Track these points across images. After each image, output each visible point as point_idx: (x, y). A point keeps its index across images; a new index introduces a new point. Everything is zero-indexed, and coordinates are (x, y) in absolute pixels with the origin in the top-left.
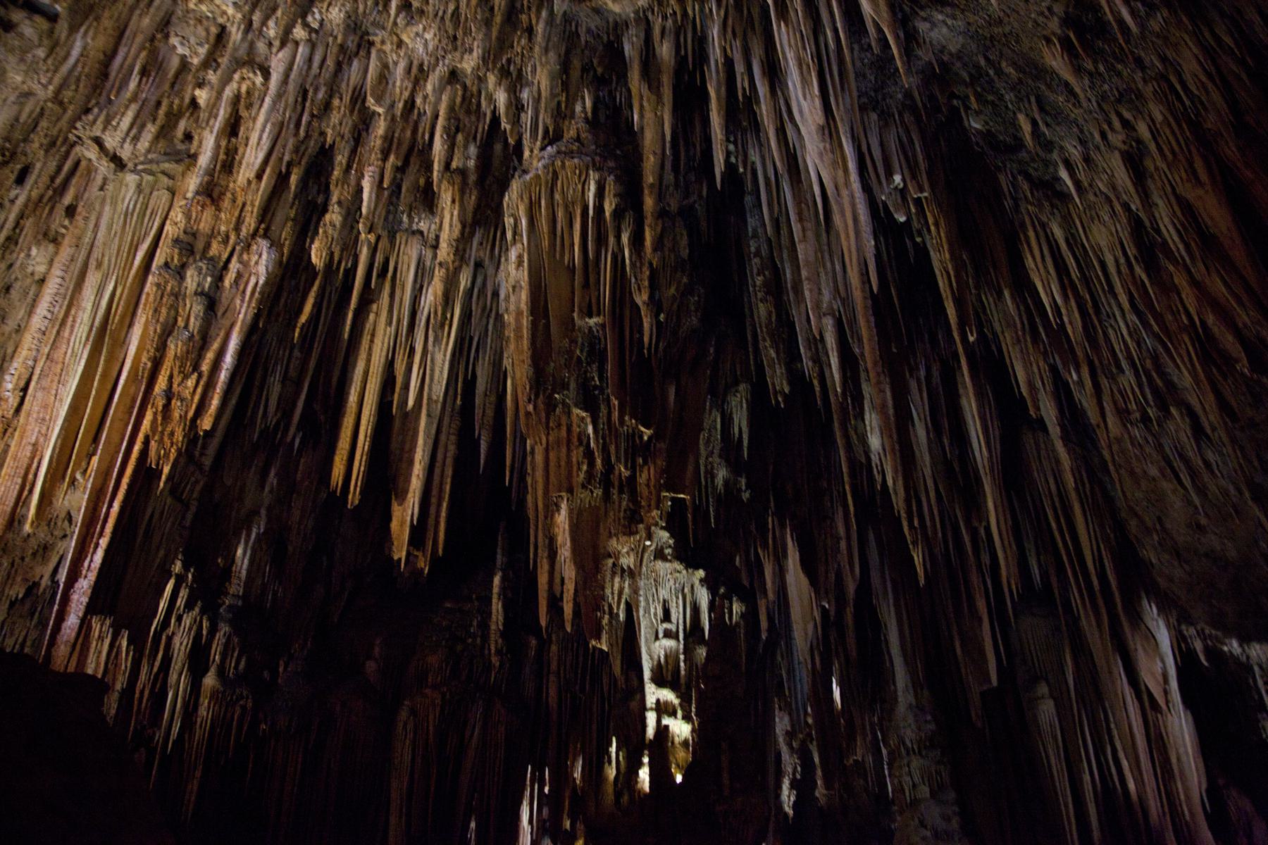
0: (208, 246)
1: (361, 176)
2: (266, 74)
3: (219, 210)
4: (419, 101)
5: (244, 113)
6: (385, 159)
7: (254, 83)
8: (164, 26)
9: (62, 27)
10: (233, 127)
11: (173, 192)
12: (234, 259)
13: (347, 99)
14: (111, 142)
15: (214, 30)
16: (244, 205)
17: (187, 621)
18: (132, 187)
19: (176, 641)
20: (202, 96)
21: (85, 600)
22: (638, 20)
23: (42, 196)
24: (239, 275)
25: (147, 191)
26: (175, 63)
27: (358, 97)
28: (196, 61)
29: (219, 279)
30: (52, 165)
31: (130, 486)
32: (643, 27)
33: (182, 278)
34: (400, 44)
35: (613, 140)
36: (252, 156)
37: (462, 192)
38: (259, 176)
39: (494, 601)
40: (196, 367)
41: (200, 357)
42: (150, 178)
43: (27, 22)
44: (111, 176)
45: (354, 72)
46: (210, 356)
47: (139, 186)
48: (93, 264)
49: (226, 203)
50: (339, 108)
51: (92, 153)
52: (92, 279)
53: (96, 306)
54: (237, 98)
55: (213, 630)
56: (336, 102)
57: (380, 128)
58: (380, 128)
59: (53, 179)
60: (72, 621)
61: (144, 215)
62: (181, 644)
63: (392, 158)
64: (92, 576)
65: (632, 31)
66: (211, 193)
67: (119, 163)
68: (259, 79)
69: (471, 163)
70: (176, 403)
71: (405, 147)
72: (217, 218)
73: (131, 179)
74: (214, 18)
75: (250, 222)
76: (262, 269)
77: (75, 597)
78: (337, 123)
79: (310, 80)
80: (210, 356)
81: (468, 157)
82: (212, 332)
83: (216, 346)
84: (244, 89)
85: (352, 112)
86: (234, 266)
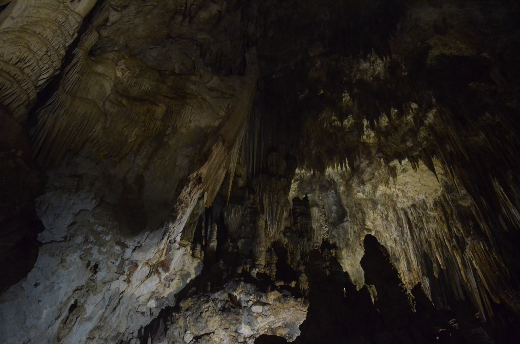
1: (436, 255)
27: (426, 239)
35: (480, 234)
37: (457, 251)
38: (418, 266)
45: (423, 236)
57: (433, 243)
58: (433, 243)
65: (472, 208)
69: (455, 243)
75: (421, 274)
76: (427, 283)
78: (425, 247)
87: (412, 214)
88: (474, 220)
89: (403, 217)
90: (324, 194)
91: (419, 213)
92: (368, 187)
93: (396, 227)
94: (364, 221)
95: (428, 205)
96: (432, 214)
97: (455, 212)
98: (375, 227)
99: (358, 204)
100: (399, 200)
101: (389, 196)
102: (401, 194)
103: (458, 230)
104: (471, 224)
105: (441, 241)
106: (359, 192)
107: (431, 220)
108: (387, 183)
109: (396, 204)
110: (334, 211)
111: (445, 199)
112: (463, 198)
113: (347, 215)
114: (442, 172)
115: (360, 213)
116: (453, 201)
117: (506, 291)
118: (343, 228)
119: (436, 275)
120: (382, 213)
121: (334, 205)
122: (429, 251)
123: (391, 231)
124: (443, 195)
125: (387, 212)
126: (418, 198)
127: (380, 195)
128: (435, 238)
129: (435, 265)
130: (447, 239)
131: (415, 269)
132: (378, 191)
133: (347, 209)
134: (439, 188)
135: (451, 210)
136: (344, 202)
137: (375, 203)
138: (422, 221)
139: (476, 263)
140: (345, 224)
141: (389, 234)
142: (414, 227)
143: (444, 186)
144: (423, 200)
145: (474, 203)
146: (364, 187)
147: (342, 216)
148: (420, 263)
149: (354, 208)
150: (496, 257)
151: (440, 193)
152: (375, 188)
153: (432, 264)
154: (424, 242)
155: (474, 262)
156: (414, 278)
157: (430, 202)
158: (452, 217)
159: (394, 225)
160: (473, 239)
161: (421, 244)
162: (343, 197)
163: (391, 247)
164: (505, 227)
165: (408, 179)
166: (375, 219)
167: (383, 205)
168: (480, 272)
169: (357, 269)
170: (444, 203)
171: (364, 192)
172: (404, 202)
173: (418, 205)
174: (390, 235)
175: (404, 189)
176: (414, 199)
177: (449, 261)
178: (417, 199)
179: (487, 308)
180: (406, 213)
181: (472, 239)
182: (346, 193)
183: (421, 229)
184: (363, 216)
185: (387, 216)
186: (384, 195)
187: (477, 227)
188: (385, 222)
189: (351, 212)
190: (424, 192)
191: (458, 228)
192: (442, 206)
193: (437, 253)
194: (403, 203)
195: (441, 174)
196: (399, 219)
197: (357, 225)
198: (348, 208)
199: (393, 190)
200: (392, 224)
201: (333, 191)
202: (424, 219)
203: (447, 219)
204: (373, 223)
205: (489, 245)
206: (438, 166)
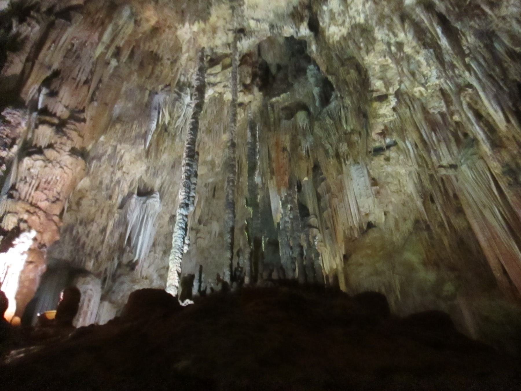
2: (470, 86)
3: (506, 148)
5: (477, 107)
7: (470, 94)
8: (424, 110)
9: (401, 144)
10: (478, 116)
11: (482, 158)
13: (508, 59)
14: (444, 163)
15: (439, 93)
16: (514, 137)
20: (456, 118)
26: (439, 117)
28: (444, 109)
30: (437, 189)
34: (504, 18)
36: (498, 117)
38: (508, 121)
42: (469, 161)
43: (391, 152)
44: (456, 173)
47: (469, 167)
48: (482, 208)
49: (506, 142)
50: (509, 65)
51: (443, 172)
54: (470, 106)
56: (506, 65)
59: (441, 191)
61: (481, 176)
66: (497, 143)
67: (453, 167)
68: (470, 90)
72: (509, 151)
73: (464, 168)
74: (435, 90)
79: (487, 69)
84: (468, 99)
90: (302, 80)
98: (388, 84)
115: (352, 71)
120: (389, 44)
121: (317, 86)
140: (333, 104)
146: (327, 6)
189: (338, 80)
197: (350, 94)
198: (332, 74)
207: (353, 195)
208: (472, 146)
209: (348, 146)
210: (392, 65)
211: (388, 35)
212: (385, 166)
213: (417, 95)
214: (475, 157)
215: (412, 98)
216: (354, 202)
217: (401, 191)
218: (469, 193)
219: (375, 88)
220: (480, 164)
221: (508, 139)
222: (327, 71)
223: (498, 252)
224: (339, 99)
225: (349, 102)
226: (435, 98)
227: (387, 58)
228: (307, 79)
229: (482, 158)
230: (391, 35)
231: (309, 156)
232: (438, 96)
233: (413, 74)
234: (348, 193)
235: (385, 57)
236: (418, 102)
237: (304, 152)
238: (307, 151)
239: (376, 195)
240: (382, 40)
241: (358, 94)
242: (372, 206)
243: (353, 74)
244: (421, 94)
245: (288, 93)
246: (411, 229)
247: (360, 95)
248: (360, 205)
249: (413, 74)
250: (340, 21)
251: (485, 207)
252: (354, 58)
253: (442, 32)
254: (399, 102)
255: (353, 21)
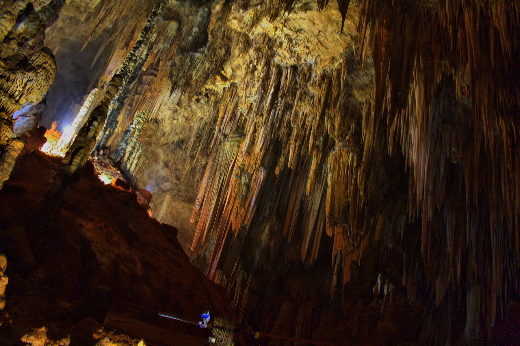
0: (248, 169)
1: (290, 147)
4: (307, 122)
6: (296, 142)
8: (236, 106)
12: (255, 173)
15: (249, 105)
17: (241, 273)
18: (228, 146)
19: (238, 279)
21: (216, 266)
22: (366, 103)
23: (205, 147)
24: (256, 178)
25: (232, 147)
27: (289, 123)
29: (250, 179)
31: (227, 236)
32: (367, 105)
33: (241, 179)
37: (317, 153)
38: (261, 150)
39: (334, 275)
40: (244, 206)
41: (245, 202)
45: (287, 117)
46: (248, 202)
52: (218, 173)
53: (219, 182)
55: (248, 276)
56: (282, 125)
58: (295, 132)
60: (213, 271)
62: (239, 280)
63: (298, 142)
64: (218, 260)
65: (364, 106)
66: (249, 152)
67: (225, 136)
69: (321, 144)
70: (239, 216)
71: (301, 139)
75: (259, 162)
76: (262, 176)
77: (214, 265)
78: (283, 131)
80: (248, 202)
81: (320, 142)
82: (249, 195)
83: (249, 199)
85: (287, 128)
86: (254, 175)
87: (286, 78)
88: (359, 124)
89: (273, 77)
90: (194, 8)
91: (296, 82)
92: (248, 16)
93: (258, 88)
94: (223, 61)
95: (313, 75)
96: (311, 90)
97: (341, 100)
98: (233, 76)
99: (228, 38)
100: (280, 51)
101: (270, 40)
102: (285, 45)
103: (333, 126)
104: (353, 127)
105: (305, 134)
106: (235, 18)
107: (307, 99)
108: (274, 17)
109: (273, 55)
110: (193, 34)
111: (338, 77)
112: (362, 88)
113: (206, 45)
114: (355, 33)
115: (223, 50)
116: (346, 84)
117: (346, 225)
118: (192, 60)
119: (277, 172)
120: (251, 62)
122: (284, 140)
123: (251, 91)
124: (339, 72)
125: (257, 62)
126: (305, 60)
127: (259, 34)
128: (300, 127)
129: (282, 159)
130: (314, 133)
131: (256, 152)
132: (259, 27)
133: (210, 37)
134: (338, 57)
135: (338, 95)
136: (211, 27)
137: (248, 43)
138: (294, 95)
139: (332, 177)
140: (198, 55)
141: (246, 94)
142: (280, 94)
143: (346, 57)
144: (311, 65)
145: (373, 103)
147: (200, 42)
148: (266, 150)
149: (219, 41)
150: (359, 179)
151: (336, 64)
152: (256, 21)
153: (280, 157)
154: (284, 125)
155: (330, 176)
156: (249, 164)
157: (318, 72)
158: (335, 106)
159: (257, 85)
160: (344, 146)
161: (280, 126)
162: (213, 19)
163: (241, 114)
164: (390, 148)
165: (305, 25)
166: (239, 67)
167: (258, 50)
168: (329, 191)
169: (191, 127)
170: (334, 80)
171: (240, 20)
172: (285, 57)
173: (300, 69)
174: (246, 96)
175: (293, 38)
176: (299, 58)
177: (302, 162)
178: (303, 61)
179: (316, 238)
180: (279, 74)
181: (343, 145)
182: (219, 16)
183: (288, 107)
184: (225, 55)
185: (255, 69)
186: (265, 35)
187: (358, 133)
188: (249, 77)
189: (212, 43)
190: (317, 54)
191: (334, 123)
192: (330, 84)
193: (292, 146)
194: (283, 58)
195: (351, 37)
196: (267, 78)
197: (211, 62)
199: (279, 33)
200: (256, 82)
201: (206, 10)
202: (298, 93)
203: (326, 106)
204: (233, 71)
205: (359, 161)
206: (354, 22)
207: (162, 100)
208: (240, 137)
209: (185, 83)
210: (243, 69)
211: (255, 59)
212: (193, 103)
213: (240, 95)
214: (237, 143)
215: (237, 94)
216: (159, 105)
217: (189, 120)
218: (219, 157)
219: (225, 70)
220: (236, 148)
221: (255, 155)
222: (212, 31)
223: (206, 195)
224: (204, 55)
225: (207, 67)
226: (246, 106)
227: (245, 65)
228: (197, 12)
229: (239, 147)
230: (256, 61)
231: (157, 55)
232: (247, 106)
233: (247, 86)
234: (160, 97)
235: (244, 63)
236: (237, 98)
237: (156, 51)
238: (158, 51)
239: (174, 111)
240: (250, 56)
241: (215, 67)
242: (167, 117)
243: (223, 52)
244: (242, 97)
245: (179, 3)
246: (175, 142)
247: (215, 68)
248: (162, 110)
249: (247, 86)
250: (242, 26)
251: (220, 169)
252: (231, 41)
253: (272, 94)
254: (229, 88)
255: (247, 33)
